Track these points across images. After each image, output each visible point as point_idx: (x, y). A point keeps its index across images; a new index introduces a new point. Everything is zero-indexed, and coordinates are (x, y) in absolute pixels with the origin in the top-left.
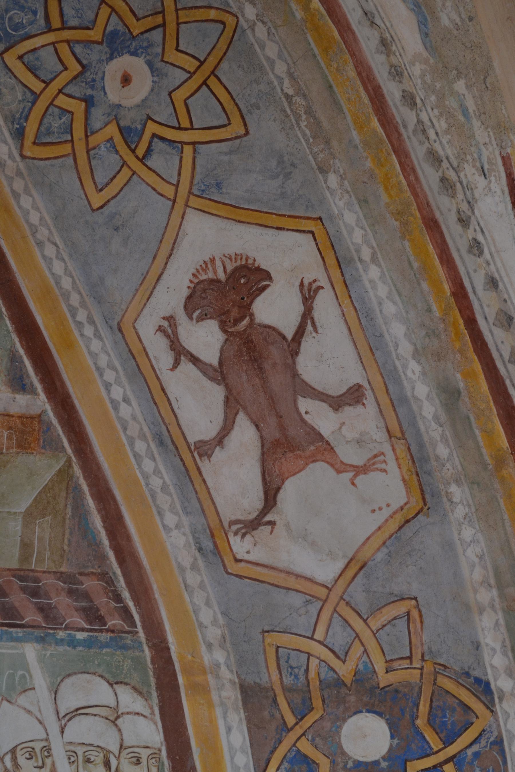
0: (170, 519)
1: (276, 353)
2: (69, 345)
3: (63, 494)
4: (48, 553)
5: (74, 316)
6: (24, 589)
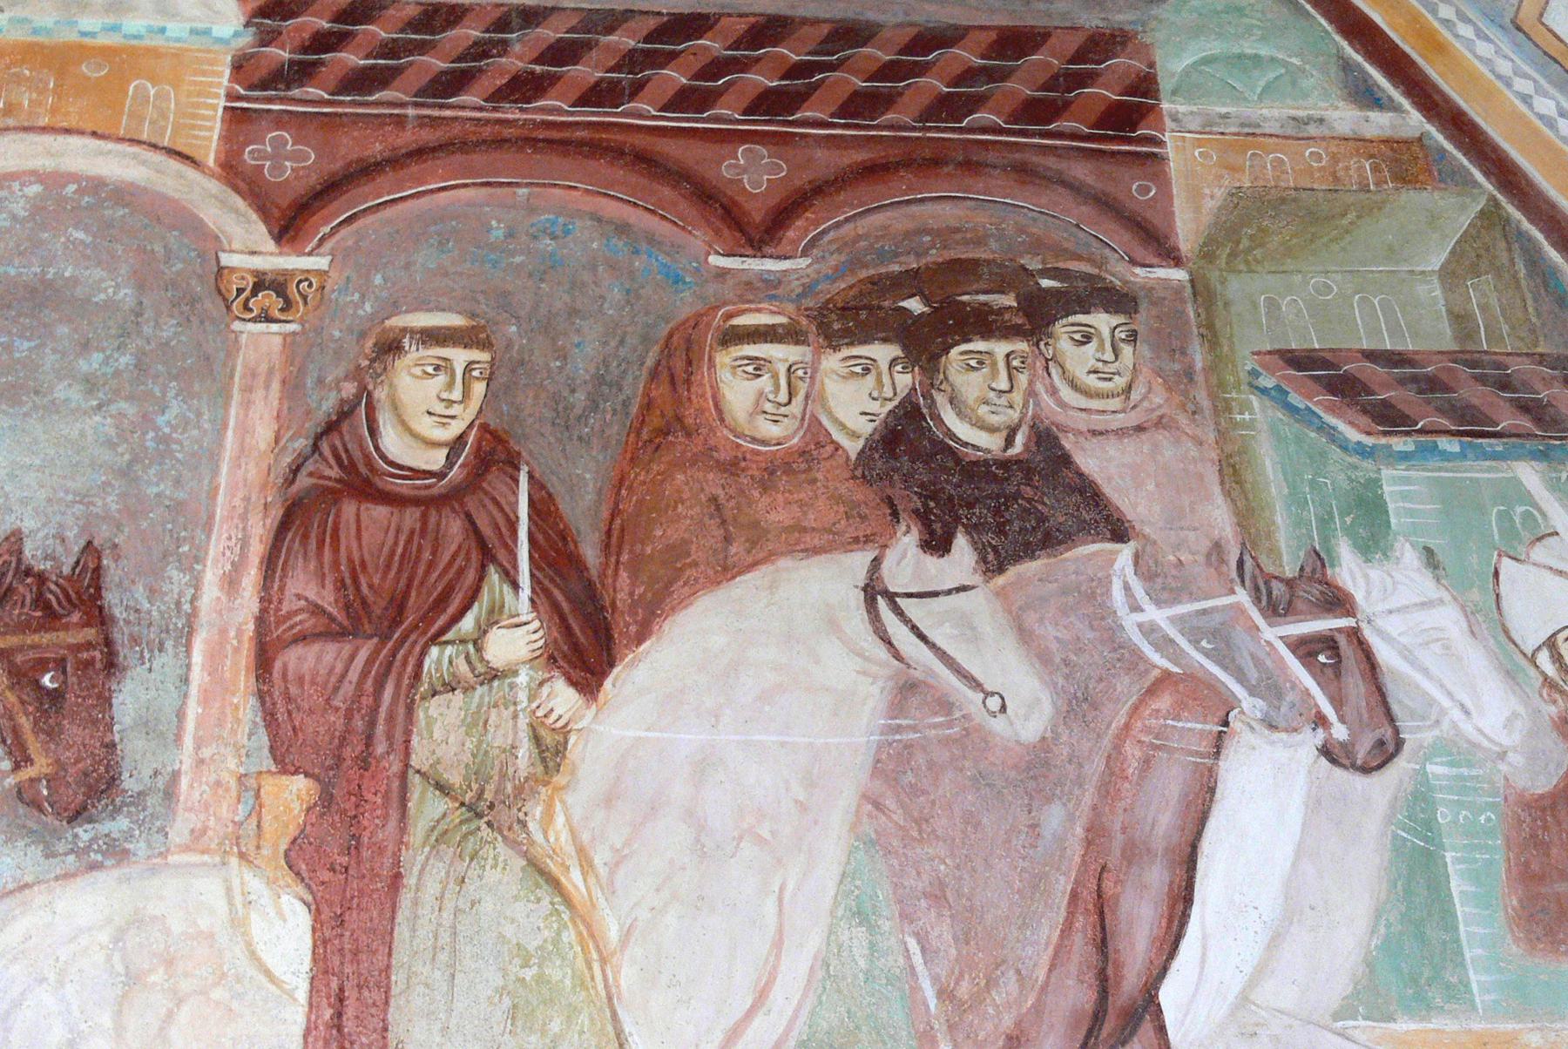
2: (1438, 48)
3: (1503, 245)
4: (1505, 328)
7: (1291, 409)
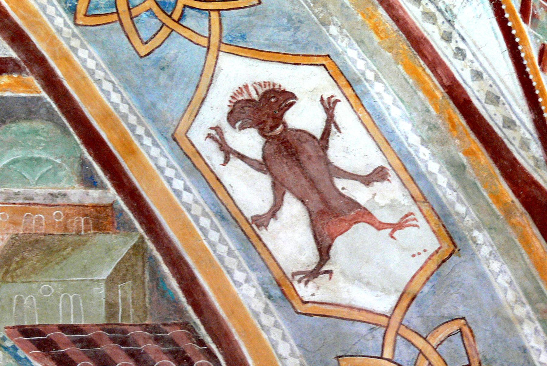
0: (239, 276)
1: (309, 148)
2: (131, 151)
3: (140, 263)
4: (132, 310)
5: (133, 131)
6: (113, 340)
7: (18, 358)
